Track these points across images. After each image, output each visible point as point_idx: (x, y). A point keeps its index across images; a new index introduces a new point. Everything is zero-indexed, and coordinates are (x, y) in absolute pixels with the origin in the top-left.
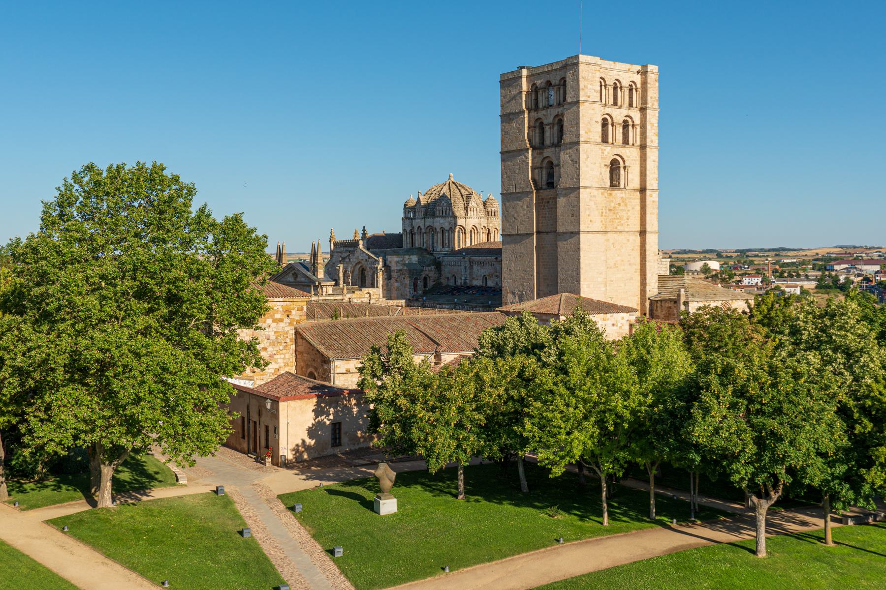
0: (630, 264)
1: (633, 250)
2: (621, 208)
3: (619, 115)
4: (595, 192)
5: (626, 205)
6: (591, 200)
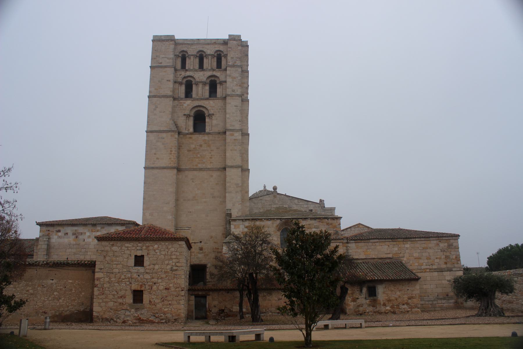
0: (213, 197)
1: (217, 184)
3: (201, 76)
4: (164, 135)
5: (209, 146)
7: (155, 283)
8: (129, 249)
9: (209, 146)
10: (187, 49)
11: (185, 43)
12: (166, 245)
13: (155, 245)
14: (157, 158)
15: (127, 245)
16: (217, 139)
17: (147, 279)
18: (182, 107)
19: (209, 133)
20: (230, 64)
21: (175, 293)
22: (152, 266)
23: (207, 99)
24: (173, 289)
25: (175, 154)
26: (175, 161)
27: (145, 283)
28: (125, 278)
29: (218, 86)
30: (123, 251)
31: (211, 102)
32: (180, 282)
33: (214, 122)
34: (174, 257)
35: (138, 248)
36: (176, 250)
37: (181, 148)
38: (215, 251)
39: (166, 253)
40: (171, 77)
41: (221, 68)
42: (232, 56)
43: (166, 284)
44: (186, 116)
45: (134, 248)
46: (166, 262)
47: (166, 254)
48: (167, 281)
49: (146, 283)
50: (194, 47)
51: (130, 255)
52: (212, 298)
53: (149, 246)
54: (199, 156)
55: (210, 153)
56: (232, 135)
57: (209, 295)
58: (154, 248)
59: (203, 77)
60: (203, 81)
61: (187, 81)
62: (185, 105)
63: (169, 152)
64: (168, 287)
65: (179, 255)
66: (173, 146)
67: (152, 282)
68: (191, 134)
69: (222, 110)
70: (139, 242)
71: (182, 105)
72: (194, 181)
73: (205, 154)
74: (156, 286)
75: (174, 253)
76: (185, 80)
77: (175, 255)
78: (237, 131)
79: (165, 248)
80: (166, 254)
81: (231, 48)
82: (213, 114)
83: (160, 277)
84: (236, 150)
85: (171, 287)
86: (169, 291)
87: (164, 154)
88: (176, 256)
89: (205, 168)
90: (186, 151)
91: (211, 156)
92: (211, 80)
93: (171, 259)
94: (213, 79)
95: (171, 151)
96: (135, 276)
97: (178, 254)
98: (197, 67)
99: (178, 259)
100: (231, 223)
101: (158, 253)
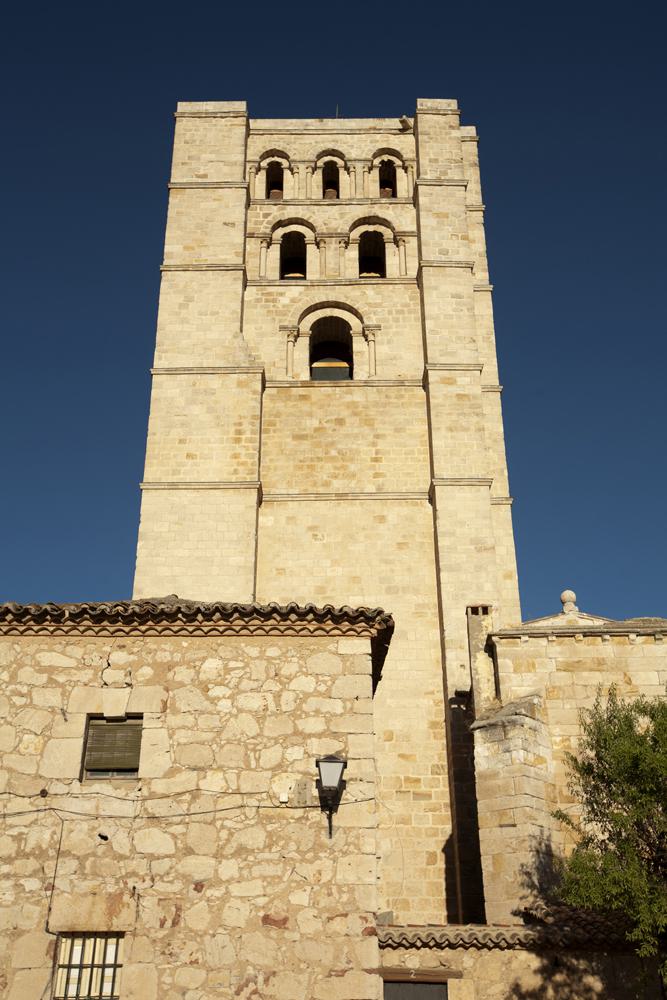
0: (389, 590)
1: (400, 546)
2: (343, 430)
4: (214, 382)
6: (192, 402)
7: (199, 887)
8: (61, 679)
9: (369, 422)
10: (285, 145)
11: (280, 130)
12: (269, 659)
13: (204, 659)
14: (188, 456)
15: (48, 658)
16: (393, 400)
17: (152, 857)
18: (274, 306)
19: (367, 384)
20: (428, 177)
21: (324, 954)
22: (185, 780)
23: (351, 283)
24: (308, 923)
25: (251, 441)
26: (252, 464)
27: (140, 886)
28: (22, 854)
29: (390, 249)
30: (25, 690)
31: (370, 291)
32: (352, 879)
33: (383, 350)
34: (314, 725)
35: (110, 675)
36: (322, 688)
37: (272, 428)
38: (403, 789)
39: (272, 707)
40: (238, 214)
41: (394, 195)
42: (432, 157)
43: (269, 890)
44: (286, 333)
45: (86, 675)
46: (271, 756)
47: (266, 708)
48: (270, 870)
49: (148, 883)
50: (308, 139)
51: (64, 712)
52: (477, 992)
53: (170, 667)
54: (334, 453)
55: (374, 444)
56: (451, 382)
57: (459, 975)
58: (202, 677)
59: (341, 222)
60: (339, 231)
61: (285, 236)
62: (285, 300)
63: (232, 435)
64: (277, 910)
65: (341, 715)
66: (244, 417)
67: (186, 878)
68: (304, 385)
69: (406, 315)
70: (120, 641)
71: (274, 301)
72: (320, 536)
73: (354, 446)
74: (208, 900)
75: (311, 704)
76: (281, 232)
77: (317, 712)
78: (467, 368)
79: (263, 678)
80: (266, 708)
81: (429, 134)
82: (379, 327)
83: (229, 850)
84: (466, 429)
85: (301, 908)
86: (287, 934)
87: (214, 443)
88: (328, 721)
89: (358, 491)
90: (289, 440)
91: (377, 453)
92: (366, 233)
93: (300, 739)
94: (371, 228)
95: (239, 432)
96: (82, 836)
97: (339, 710)
98: (317, 192)
99: (335, 735)
100: (499, 649)
101: (225, 705)
